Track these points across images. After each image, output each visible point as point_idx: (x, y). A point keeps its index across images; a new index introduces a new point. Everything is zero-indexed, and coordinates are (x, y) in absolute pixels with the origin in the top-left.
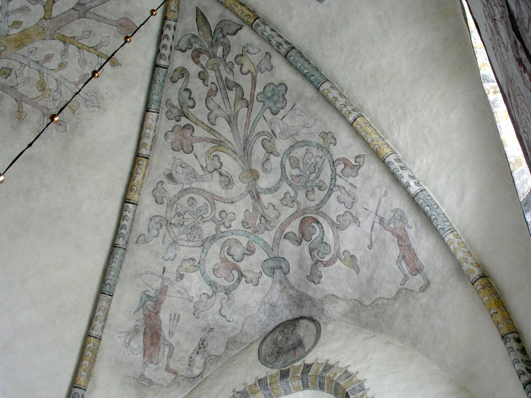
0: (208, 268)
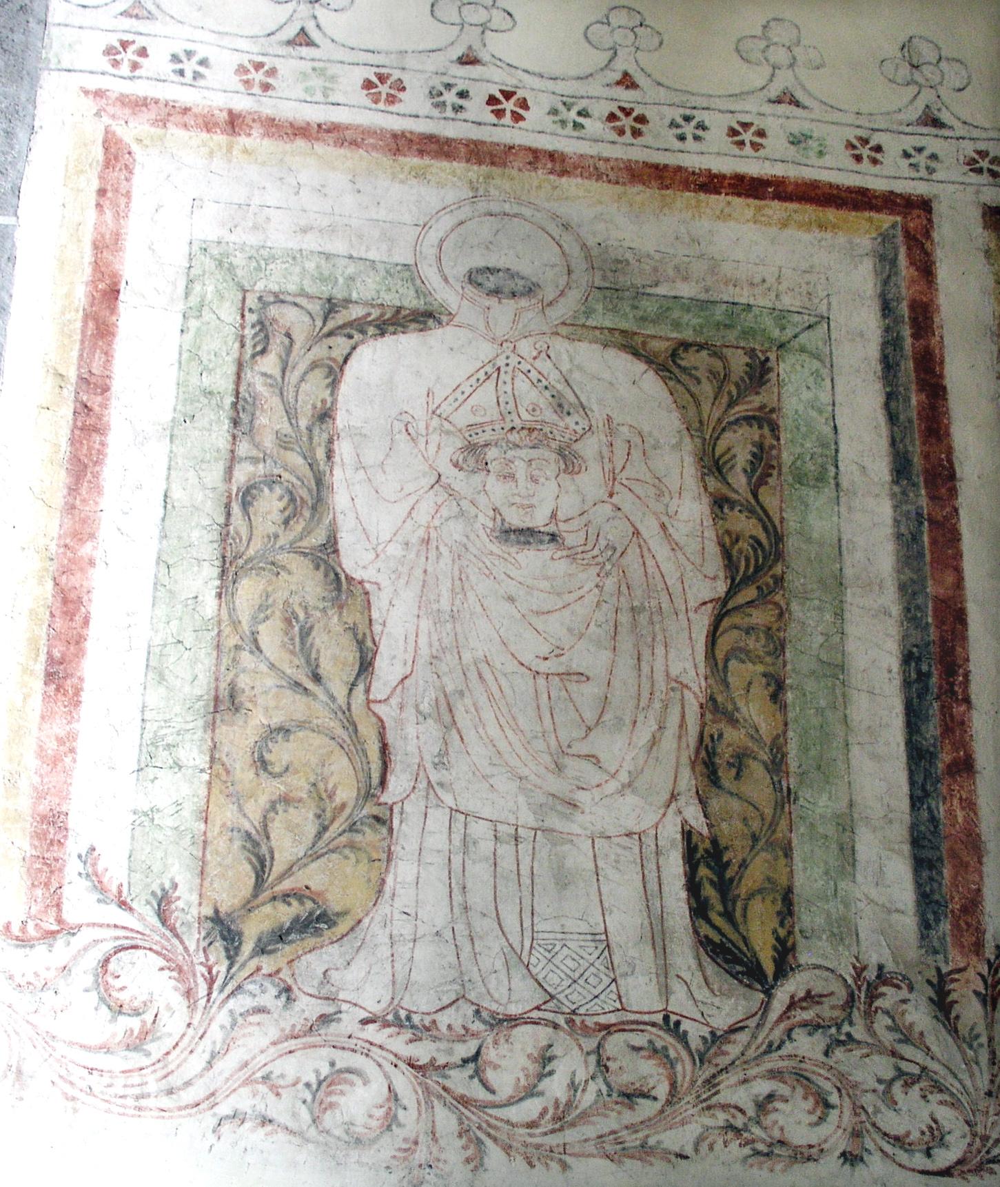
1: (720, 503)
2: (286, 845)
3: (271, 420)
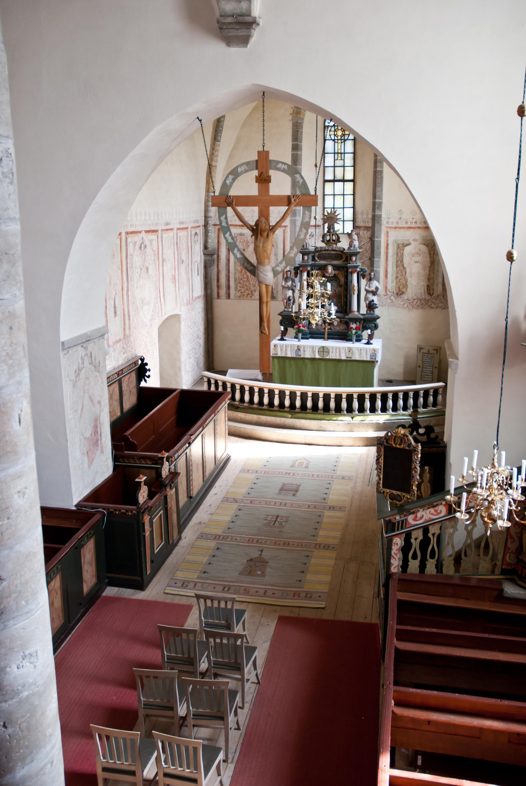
1: (430, 257)
2: (401, 288)
3: (399, 255)
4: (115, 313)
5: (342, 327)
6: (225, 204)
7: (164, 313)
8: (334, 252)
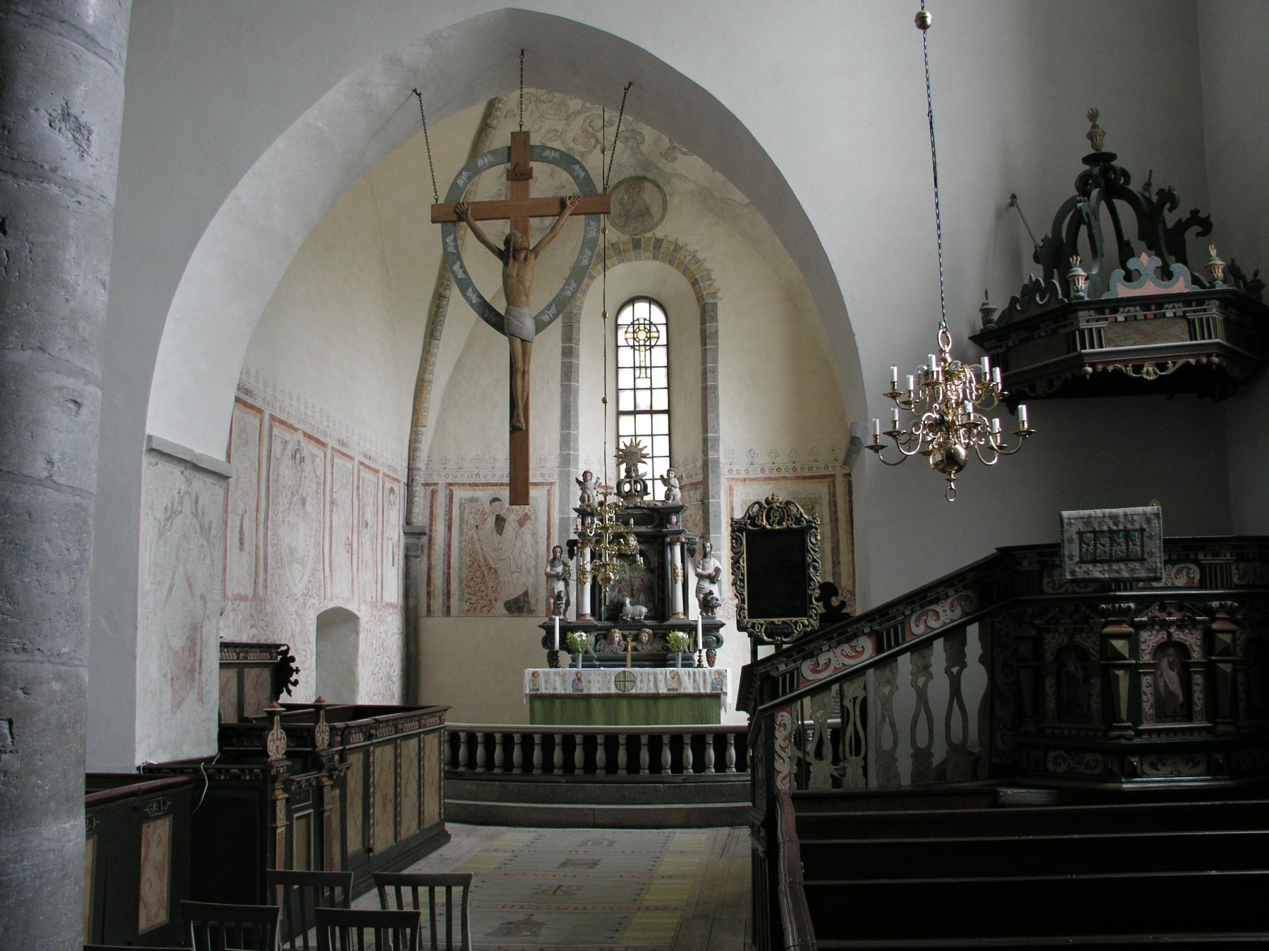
0: (569, 137)
4: (242, 543)
5: (657, 645)
6: (454, 217)
7: (328, 595)
8: (639, 512)
